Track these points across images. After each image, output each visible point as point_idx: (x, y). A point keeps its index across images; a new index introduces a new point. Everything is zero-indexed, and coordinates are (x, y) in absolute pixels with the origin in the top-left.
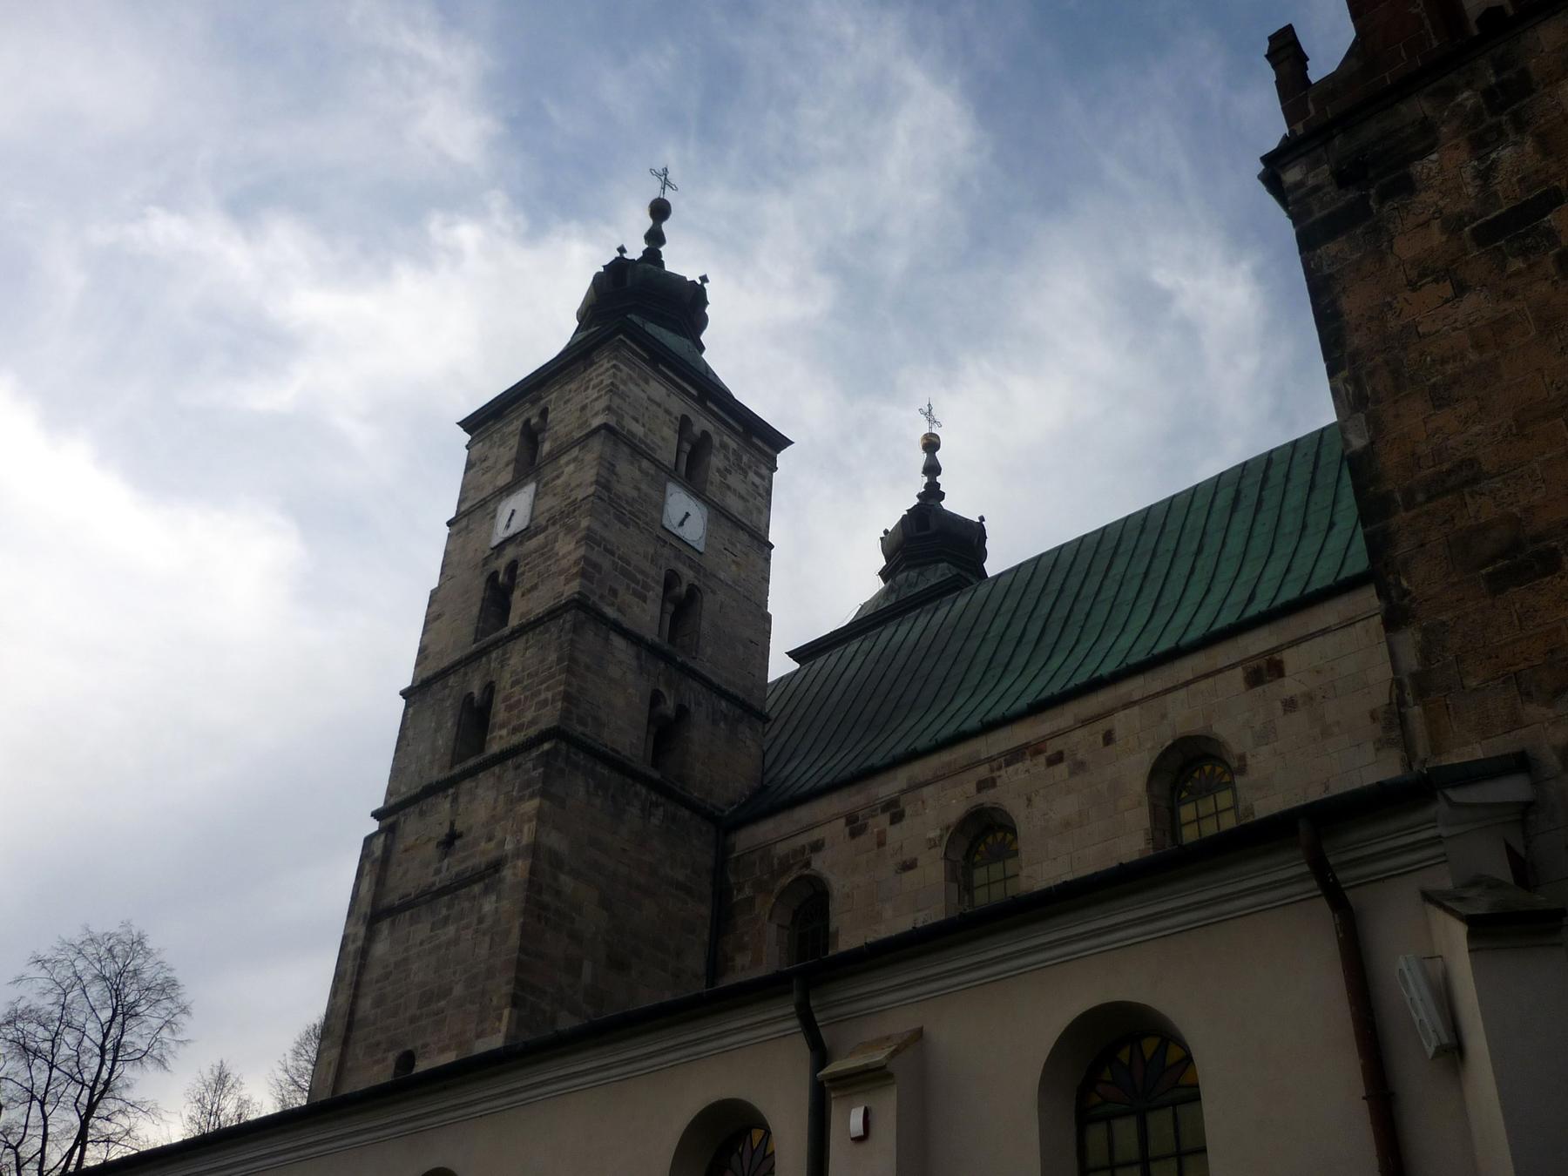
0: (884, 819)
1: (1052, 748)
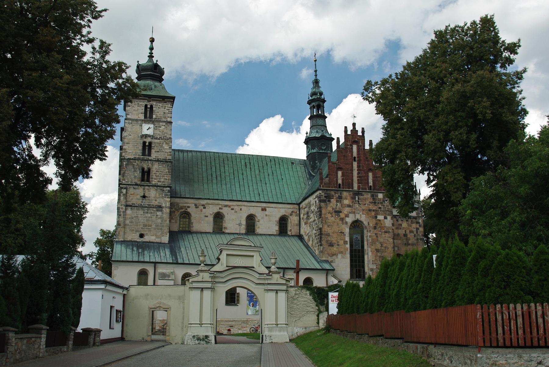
0: (202, 207)
1: (232, 207)
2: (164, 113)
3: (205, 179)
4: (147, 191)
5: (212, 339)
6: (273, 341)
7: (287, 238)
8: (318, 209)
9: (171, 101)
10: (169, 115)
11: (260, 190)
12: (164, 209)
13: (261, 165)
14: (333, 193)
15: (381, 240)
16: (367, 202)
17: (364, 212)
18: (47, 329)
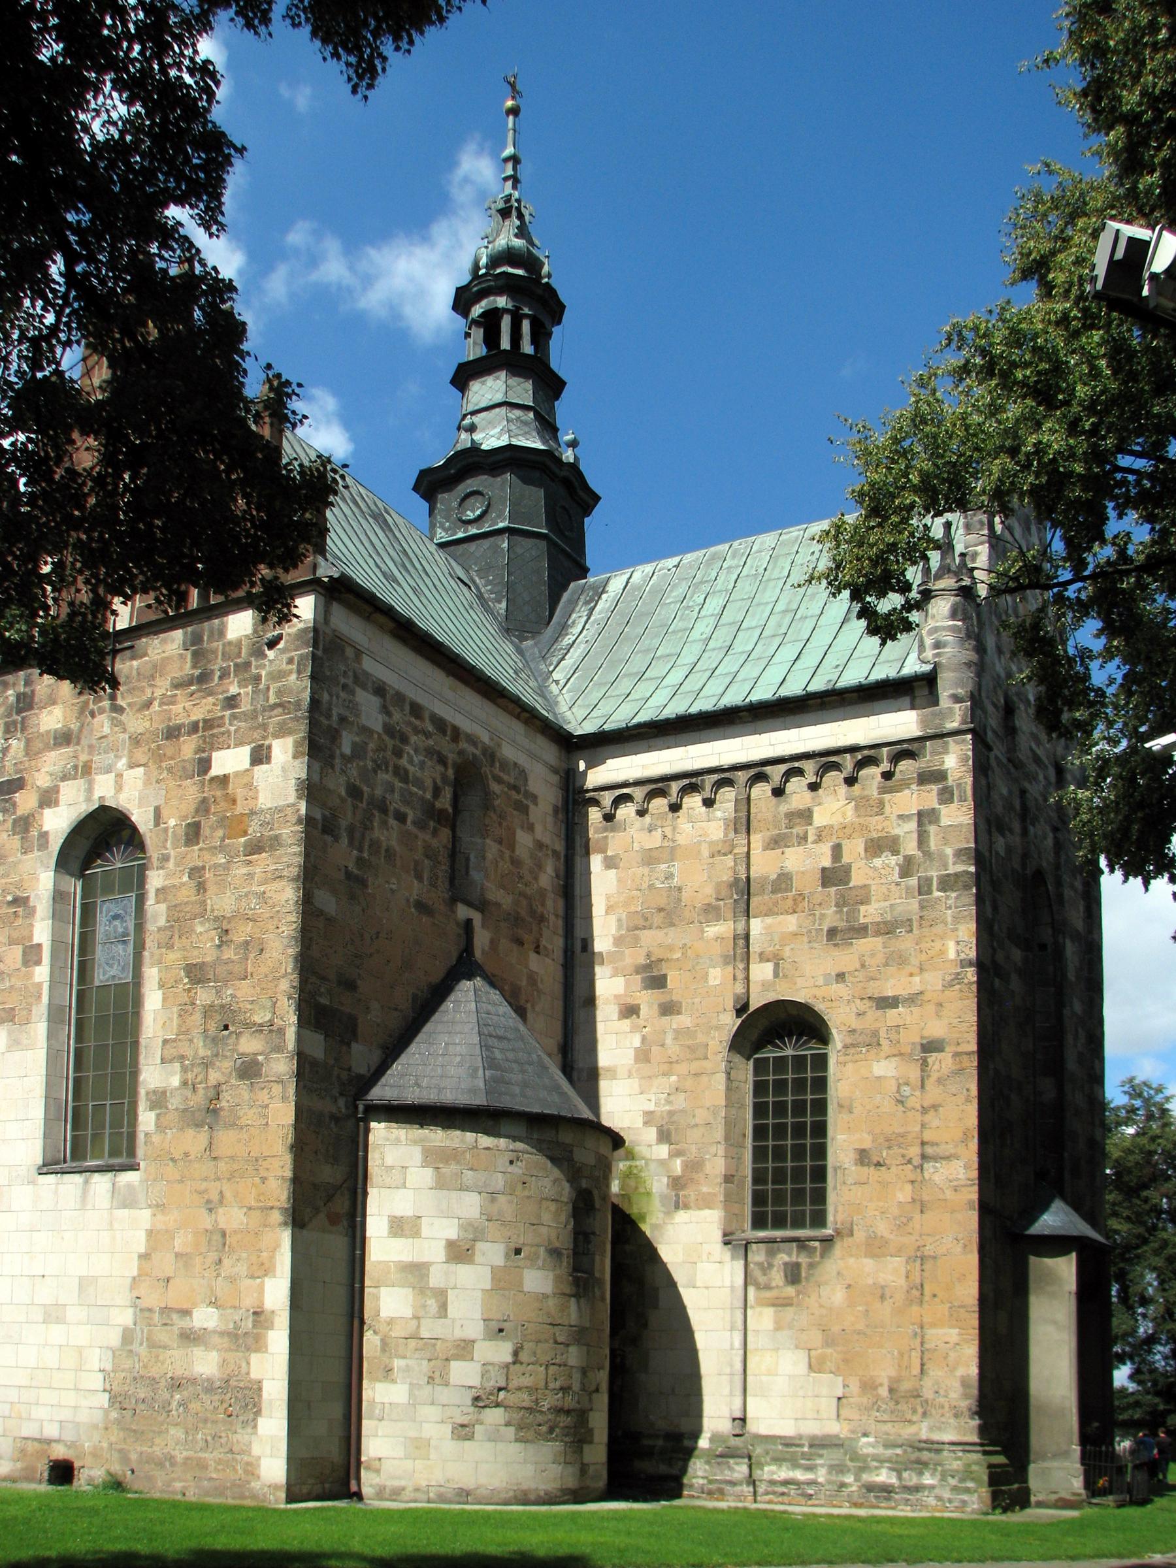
15: (223, 902)
16: (162, 686)
17: (141, 755)
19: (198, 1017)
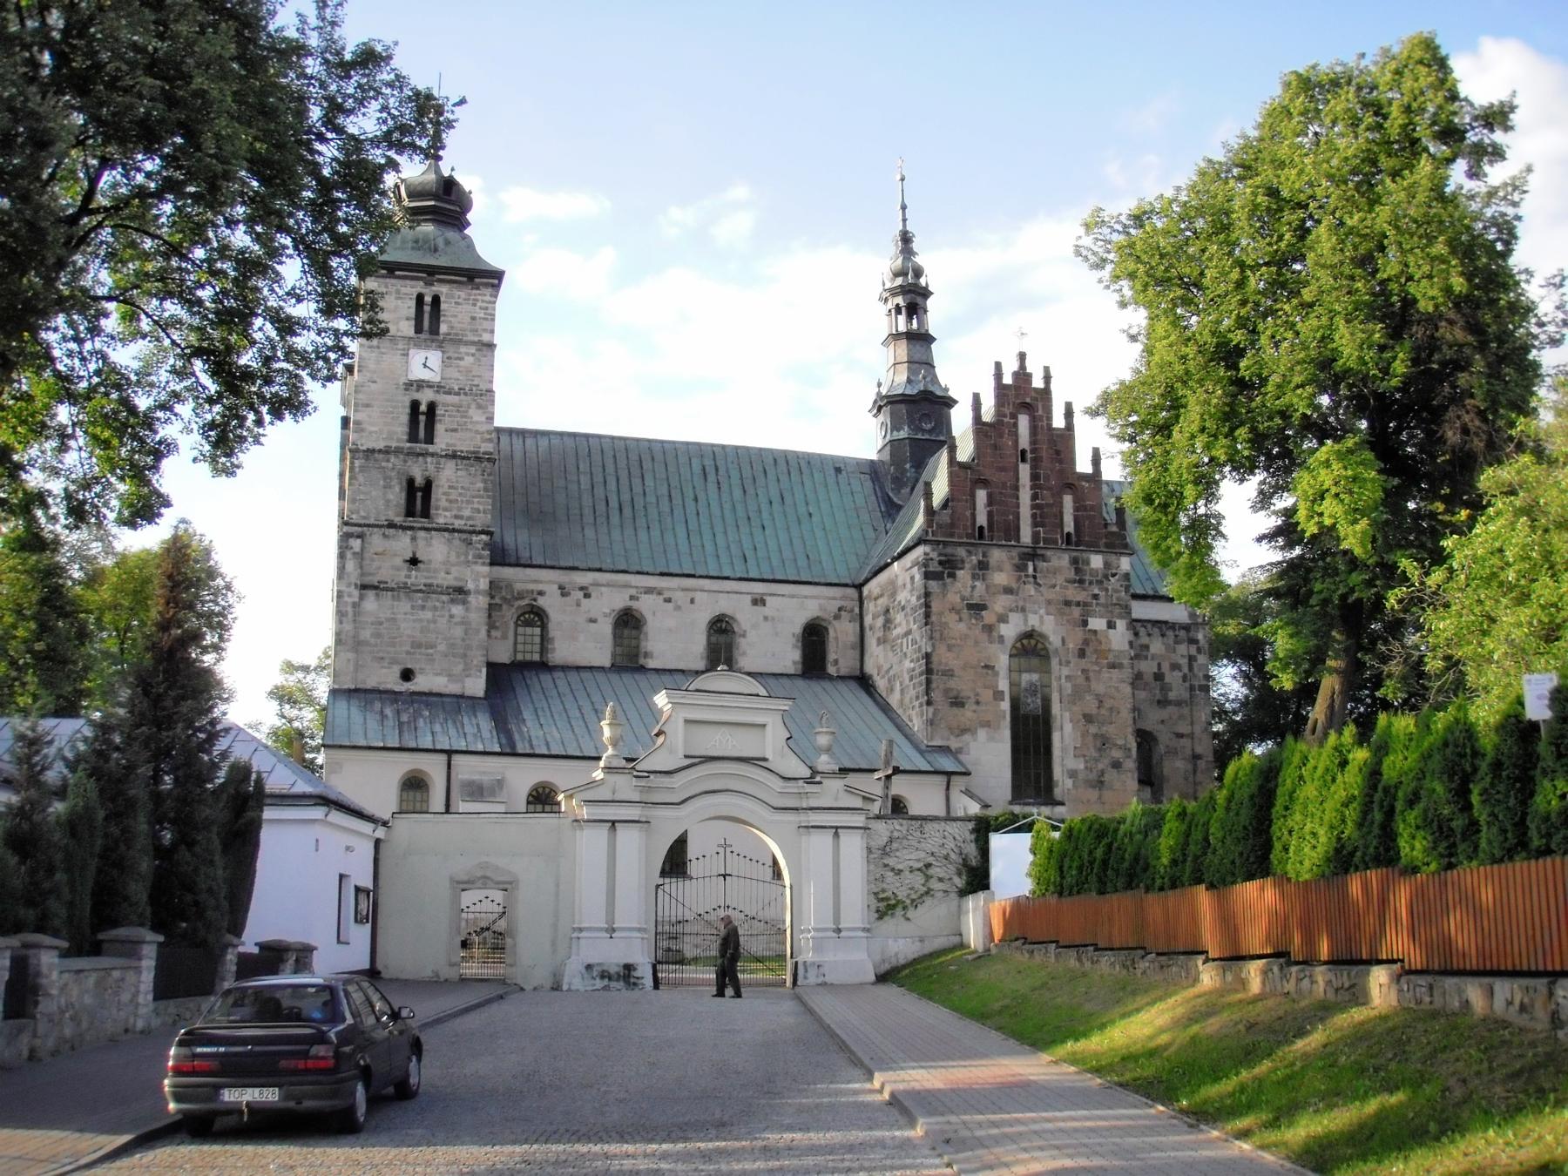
0: (581, 594)
1: (666, 595)
2: (473, 318)
3: (587, 511)
4: (421, 543)
5: (645, 972)
6: (828, 979)
7: (827, 685)
8: (918, 598)
9: (493, 286)
10: (486, 325)
11: (747, 545)
12: (471, 599)
13: (747, 473)
14: (961, 552)
15: (1099, 688)
17: (1052, 609)
18: (160, 944)
19: (1090, 738)
